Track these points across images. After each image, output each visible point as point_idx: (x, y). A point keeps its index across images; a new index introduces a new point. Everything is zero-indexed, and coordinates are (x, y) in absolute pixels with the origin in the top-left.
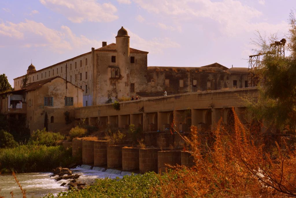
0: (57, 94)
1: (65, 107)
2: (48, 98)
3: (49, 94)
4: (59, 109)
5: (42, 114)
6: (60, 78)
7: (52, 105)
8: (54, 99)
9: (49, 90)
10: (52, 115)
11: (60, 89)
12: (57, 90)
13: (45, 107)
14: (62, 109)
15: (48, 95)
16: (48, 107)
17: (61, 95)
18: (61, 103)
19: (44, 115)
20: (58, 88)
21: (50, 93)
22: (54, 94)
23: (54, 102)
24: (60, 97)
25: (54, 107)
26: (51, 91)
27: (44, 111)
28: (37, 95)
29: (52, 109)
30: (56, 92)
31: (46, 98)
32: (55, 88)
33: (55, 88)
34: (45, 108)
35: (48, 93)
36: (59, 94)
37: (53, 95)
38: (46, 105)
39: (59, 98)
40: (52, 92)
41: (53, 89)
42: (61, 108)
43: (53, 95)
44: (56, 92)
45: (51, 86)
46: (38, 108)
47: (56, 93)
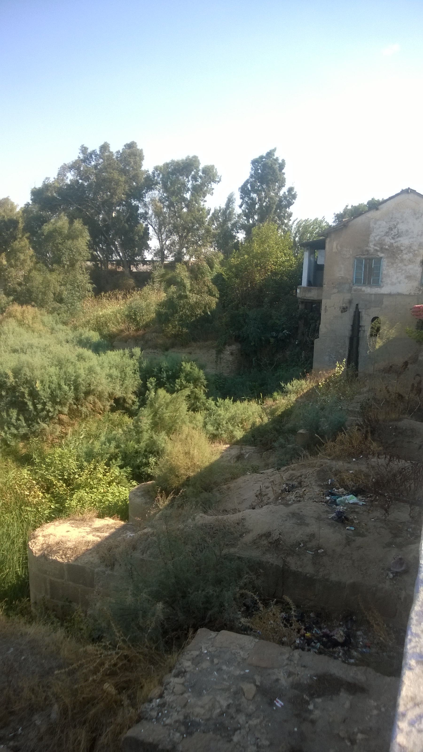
0: (397, 247)
1: (420, 290)
2: (366, 259)
3: (372, 247)
4: (399, 294)
5: (344, 310)
6: (411, 196)
7: (377, 283)
8: (385, 263)
9: (374, 234)
10: (374, 312)
11: (407, 231)
12: (399, 235)
13: (355, 287)
14: (409, 295)
15: (367, 251)
16: (364, 288)
17: (409, 252)
18: (409, 277)
19: (352, 311)
20: (402, 227)
21: (375, 245)
22: (387, 247)
23: (385, 272)
24: (405, 256)
25: (385, 290)
26: (377, 238)
27: (350, 302)
28: (335, 250)
29: (375, 294)
30: (393, 241)
31: (359, 261)
32: (391, 229)
33: (391, 229)
34: (355, 291)
35: (367, 246)
36: (402, 248)
37: (383, 253)
38: (358, 281)
39: (402, 260)
40: (381, 244)
41: (383, 233)
42: (407, 293)
43: (382, 250)
44: (393, 241)
45: (379, 223)
46: (335, 290)
47: (395, 245)
